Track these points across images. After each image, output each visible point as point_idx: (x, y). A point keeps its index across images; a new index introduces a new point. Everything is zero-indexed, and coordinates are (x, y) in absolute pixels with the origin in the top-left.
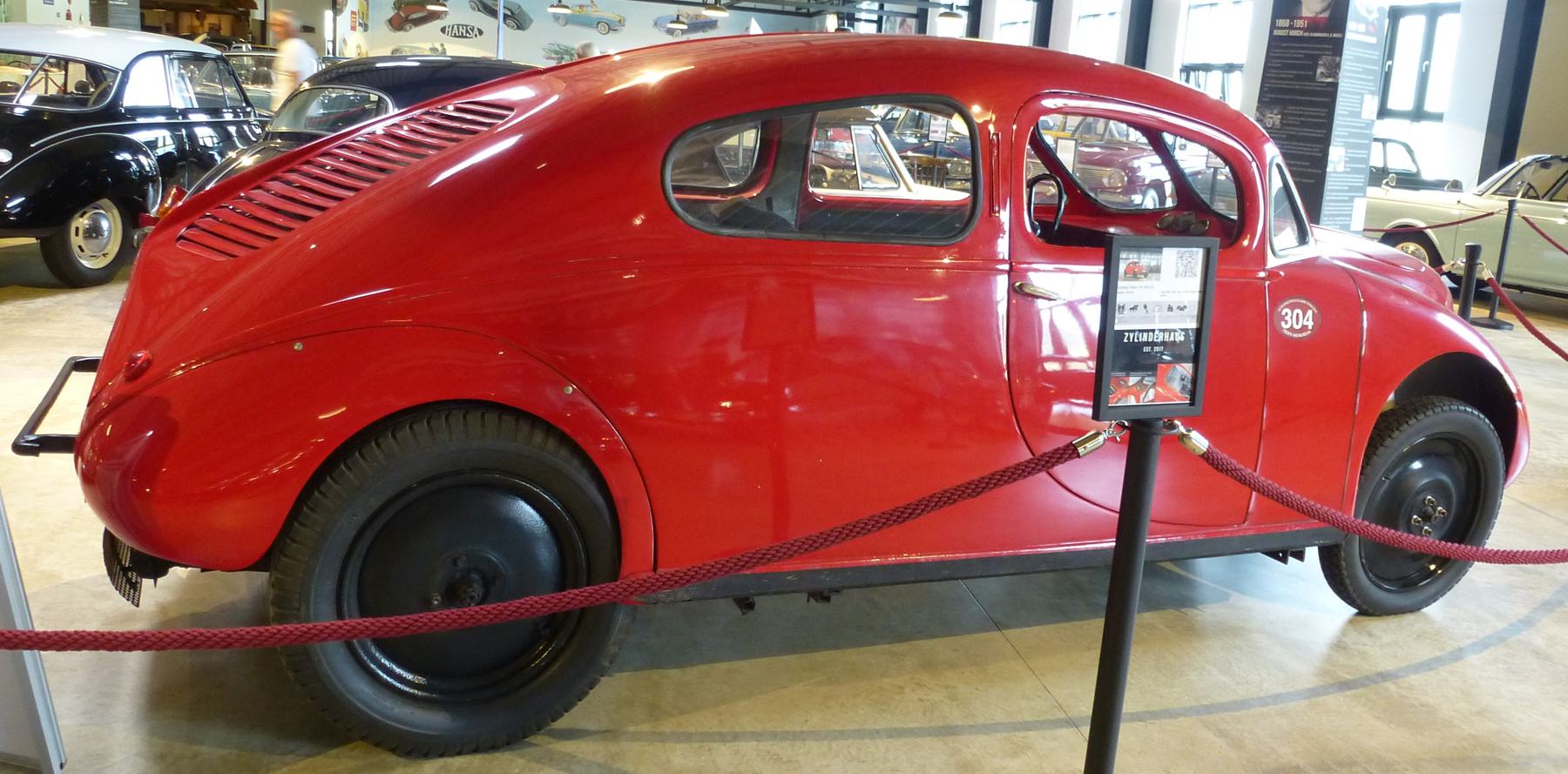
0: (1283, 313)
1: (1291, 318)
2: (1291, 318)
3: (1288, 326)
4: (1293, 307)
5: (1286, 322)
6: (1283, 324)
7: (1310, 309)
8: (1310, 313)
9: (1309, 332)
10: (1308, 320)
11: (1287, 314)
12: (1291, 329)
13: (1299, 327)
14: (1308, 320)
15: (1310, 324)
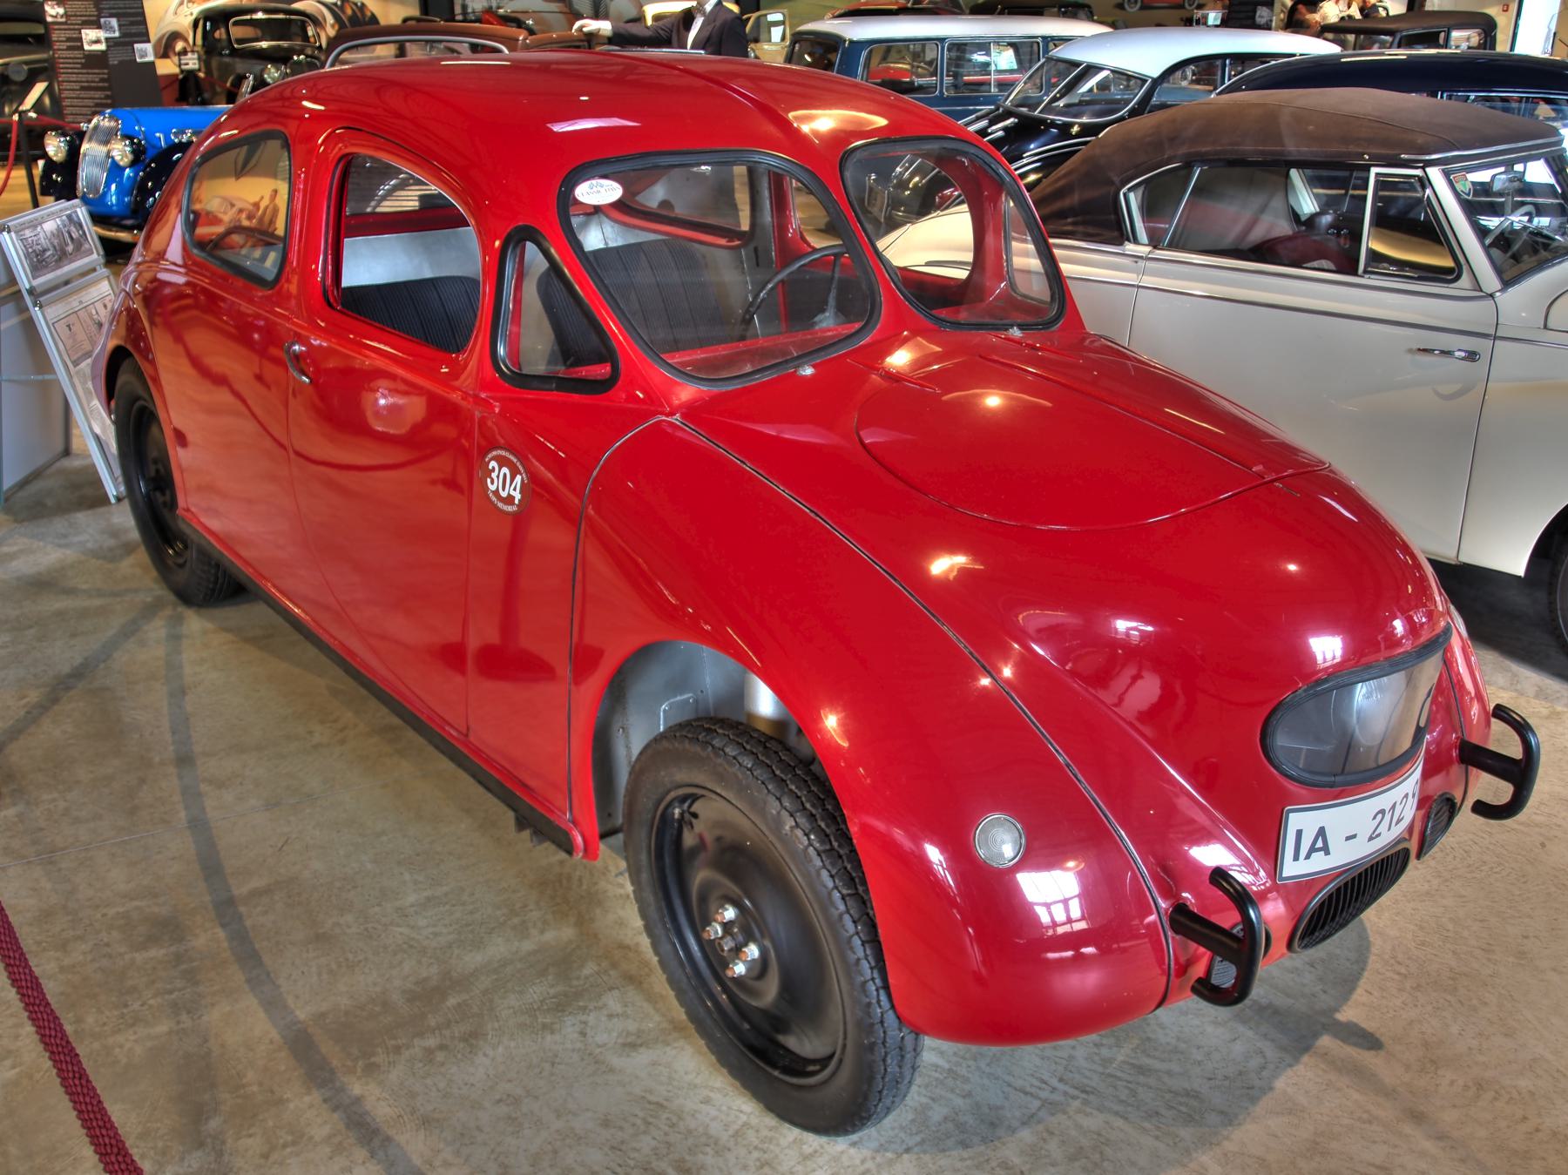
0: (490, 467)
1: (498, 477)
2: (498, 477)
3: (493, 488)
4: (502, 462)
5: (492, 483)
6: (489, 480)
7: (521, 474)
8: (518, 478)
9: (515, 508)
10: (515, 489)
11: (494, 468)
12: (496, 493)
13: (504, 494)
14: (515, 489)
15: (517, 496)
